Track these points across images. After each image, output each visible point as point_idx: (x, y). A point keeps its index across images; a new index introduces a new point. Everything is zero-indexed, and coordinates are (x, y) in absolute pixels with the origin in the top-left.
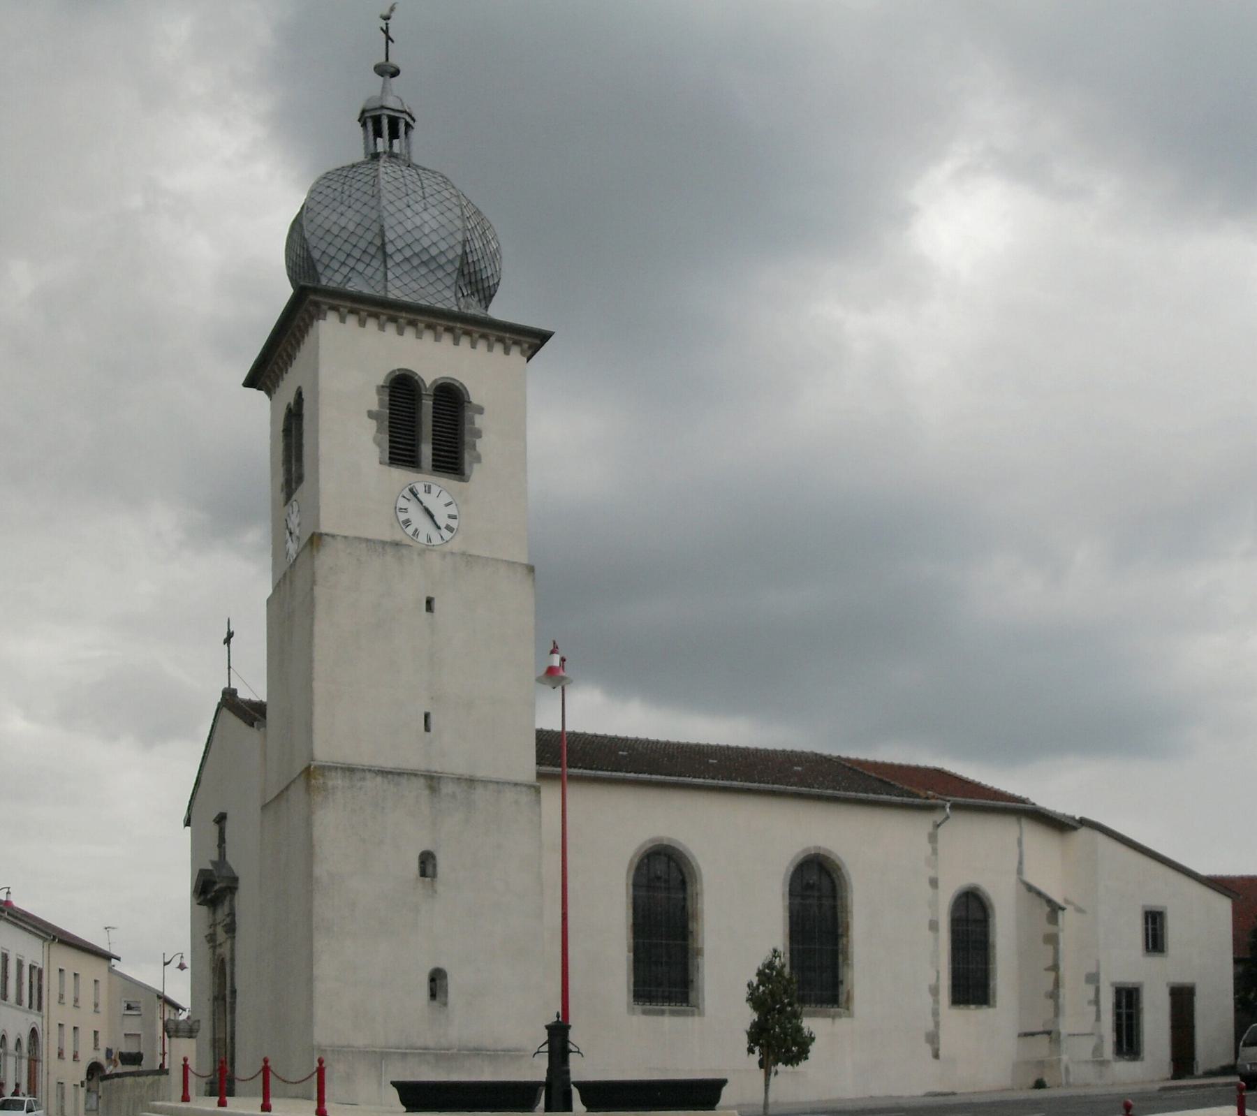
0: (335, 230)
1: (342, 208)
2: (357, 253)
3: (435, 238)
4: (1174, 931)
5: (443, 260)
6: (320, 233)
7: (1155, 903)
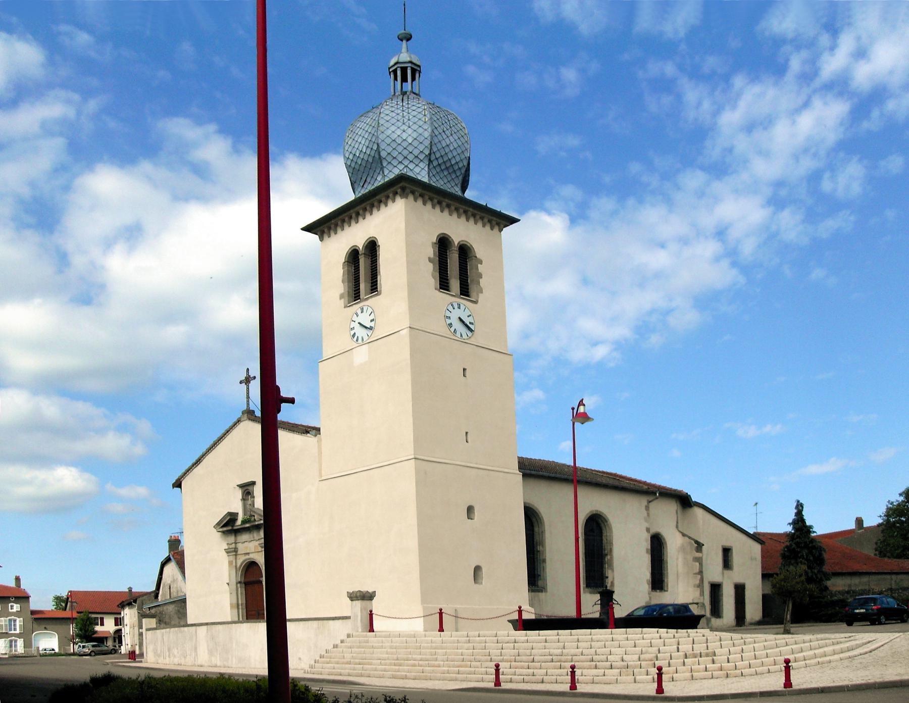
0: (399, 141)
1: (405, 127)
2: (411, 157)
3: (455, 153)
4: (736, 559)
5: (456, 167)
6: (388, 141)
7: (727, 544)
